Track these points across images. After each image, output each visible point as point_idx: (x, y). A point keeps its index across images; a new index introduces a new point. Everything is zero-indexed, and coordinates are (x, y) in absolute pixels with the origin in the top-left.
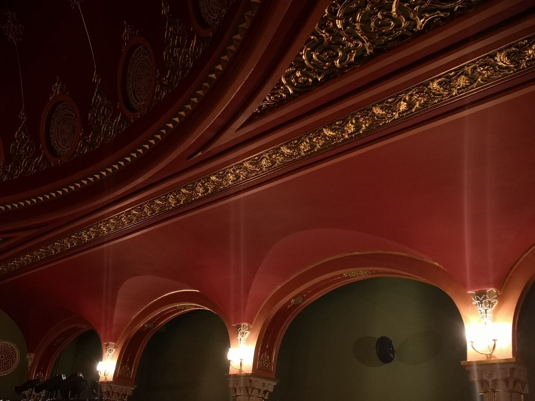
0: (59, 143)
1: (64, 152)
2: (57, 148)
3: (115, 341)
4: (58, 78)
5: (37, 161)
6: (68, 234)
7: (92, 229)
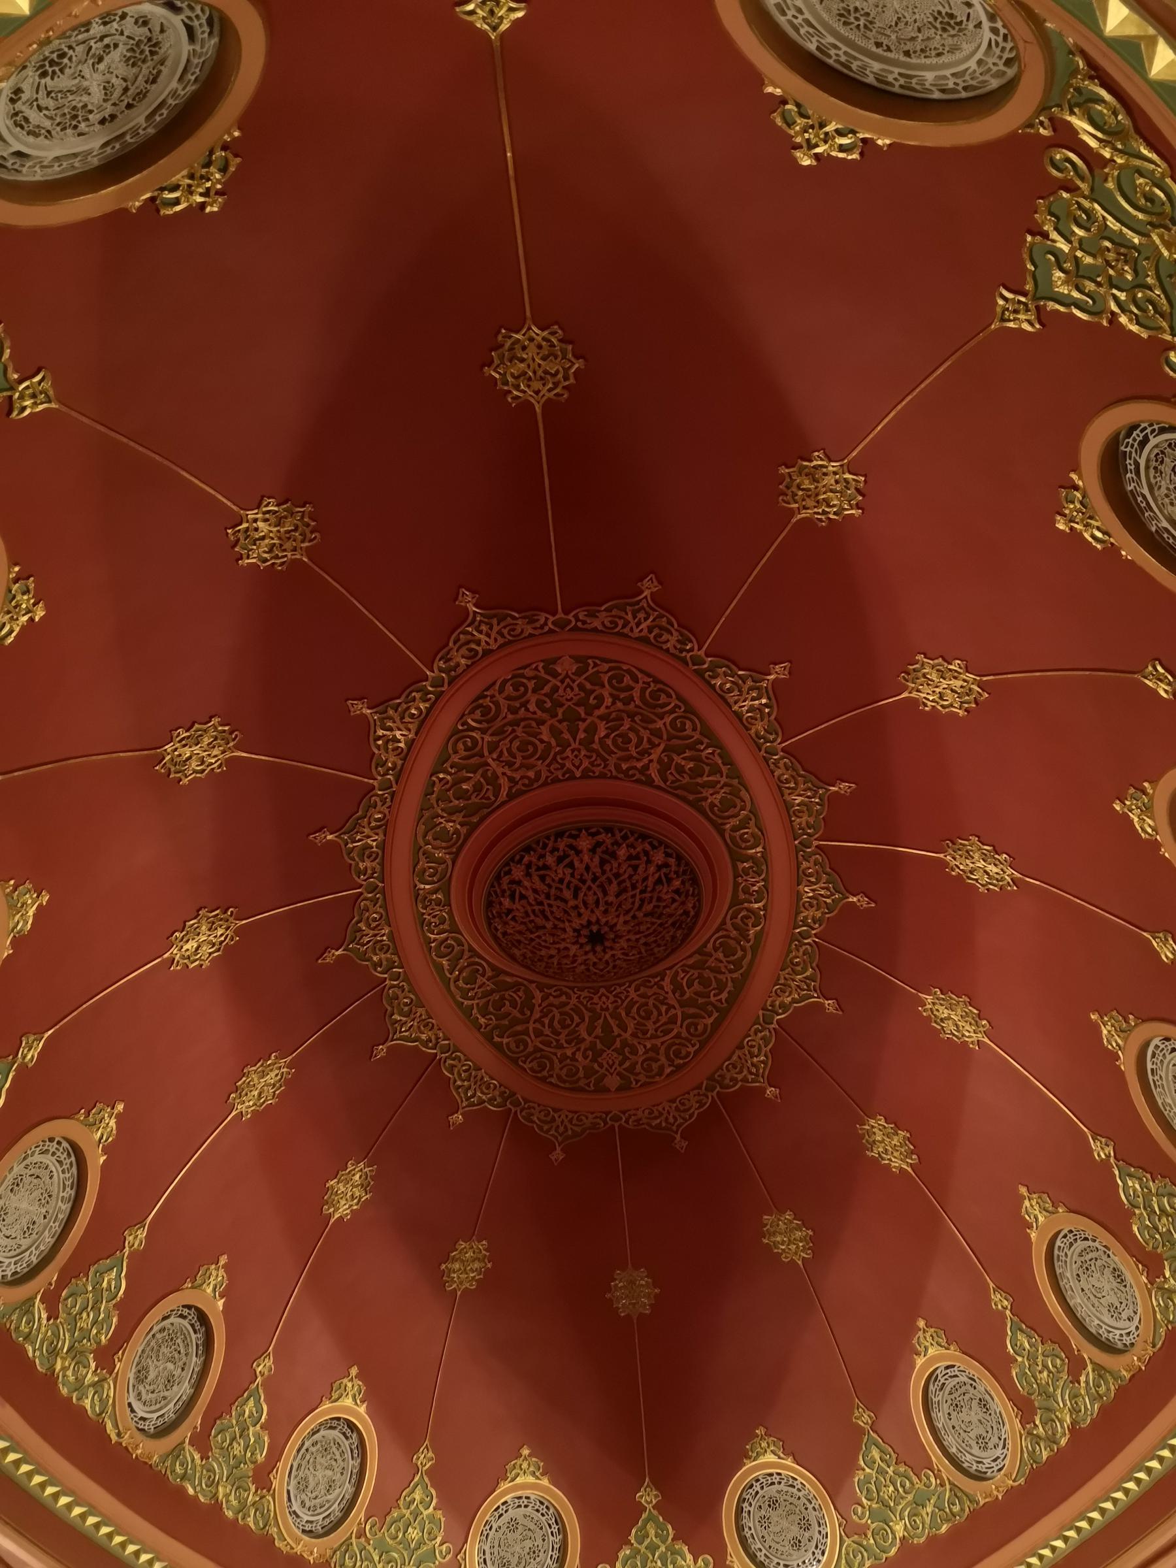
0: (1106, 1320)
1: (1128, 1334)
2: (1109, 1332)
5: (1087, 1382)
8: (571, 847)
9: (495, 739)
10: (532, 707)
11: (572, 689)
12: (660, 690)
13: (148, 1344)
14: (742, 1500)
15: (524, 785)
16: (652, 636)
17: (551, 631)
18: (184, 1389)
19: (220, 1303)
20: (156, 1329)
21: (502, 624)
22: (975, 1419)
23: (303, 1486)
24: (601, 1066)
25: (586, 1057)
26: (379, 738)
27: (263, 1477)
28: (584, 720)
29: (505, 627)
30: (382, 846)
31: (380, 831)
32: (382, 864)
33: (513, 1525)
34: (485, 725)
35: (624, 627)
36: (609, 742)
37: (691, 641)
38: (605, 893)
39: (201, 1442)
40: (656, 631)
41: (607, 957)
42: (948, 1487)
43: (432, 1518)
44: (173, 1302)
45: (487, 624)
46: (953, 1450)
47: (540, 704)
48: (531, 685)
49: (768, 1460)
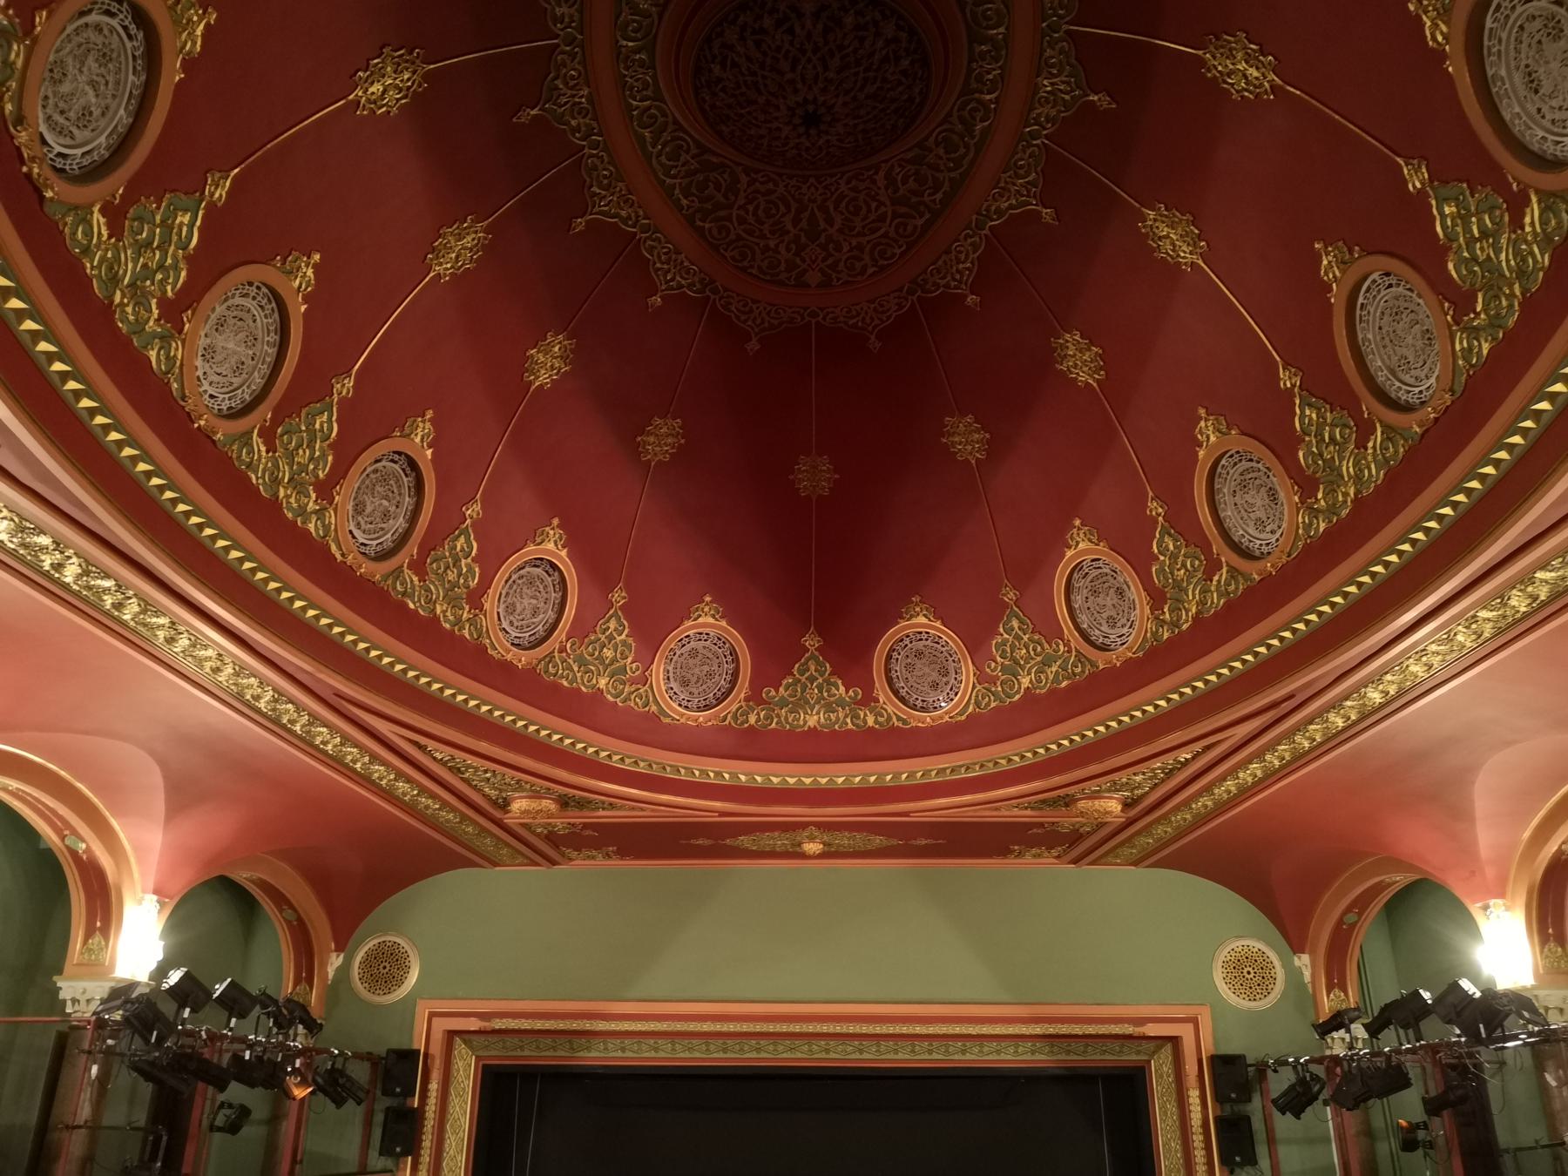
3: (1502, 895)
4: (1202, 412)
6: (1335, 705)
7: (1389, 677)
14: (892, 650)
18: (400, 523)
19: (429, 452)
22: (1109, 602)
23: (510, 610)
24: (804, 261)
25: (788, 250)
27: (475, 599)
32: (581, 12)
33: (694, 653)
39: (419, 567)
43: (624, 643)
44: (383, 447)
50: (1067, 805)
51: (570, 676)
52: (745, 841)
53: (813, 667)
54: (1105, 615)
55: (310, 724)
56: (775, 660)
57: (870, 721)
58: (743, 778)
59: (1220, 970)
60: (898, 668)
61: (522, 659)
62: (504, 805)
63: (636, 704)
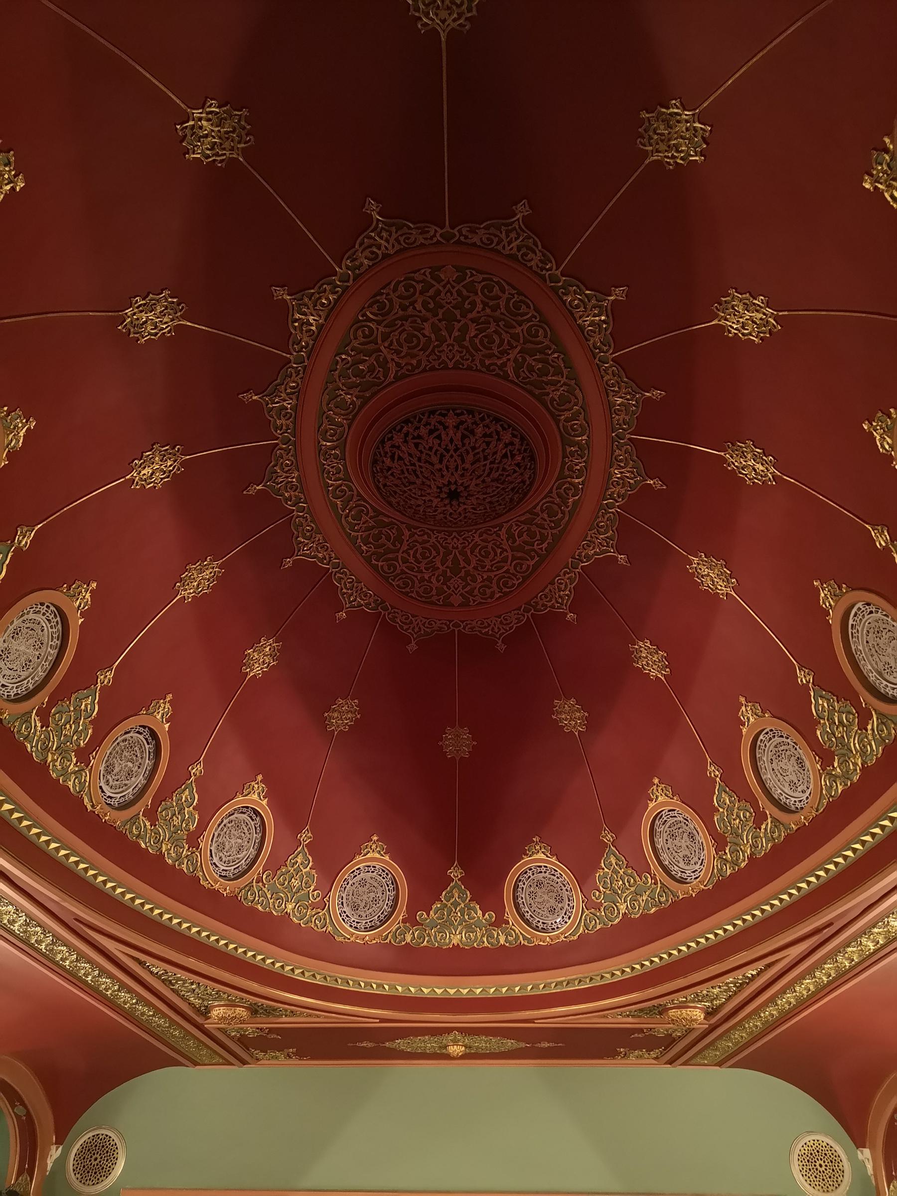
8: (440, 423)
9: (388, 330)
10: (418, 306)
11: (452, 294)
12: (521, 301)
13: (114, 749)
14: (518, 880)
15: (408, 370)
16: (519, 255)
17: (438, 242)
18: (140, 780)
19: (167, 726)
20: (119, 739)
21: (399, 233)
23: (221, 847)
24: (449, 588)
26: (296, 320)
27: (193, 840)
28: (459, 321)
29: (401, 235)
30: (295, 408)
31: (294, 397)
32: (294, 423)
34: (380, 318)
35: (498, 244)
36: (477, 341)
37: (551, 262)
38: (463, 461)
39: (151, 814)
40: (524, 250)
41: (460, 509)
42: (659, 885)
45: (387, 231)
46: (667, 863)
47: (425, 304)
48: (419, 287)
49: (539, 857)
50: (660, 1013)
51: (264, 901)
52: (401, 1044)
53: (456, 894)
54: (681, 854)
55: (53, 943)
56: (426, 890)
57: (502, 942)
58: (399, 988)
59: (796, 1163)
60: (523, 896)
61: (227, 888)
62: (205, 1012)
63: (316, 925)
